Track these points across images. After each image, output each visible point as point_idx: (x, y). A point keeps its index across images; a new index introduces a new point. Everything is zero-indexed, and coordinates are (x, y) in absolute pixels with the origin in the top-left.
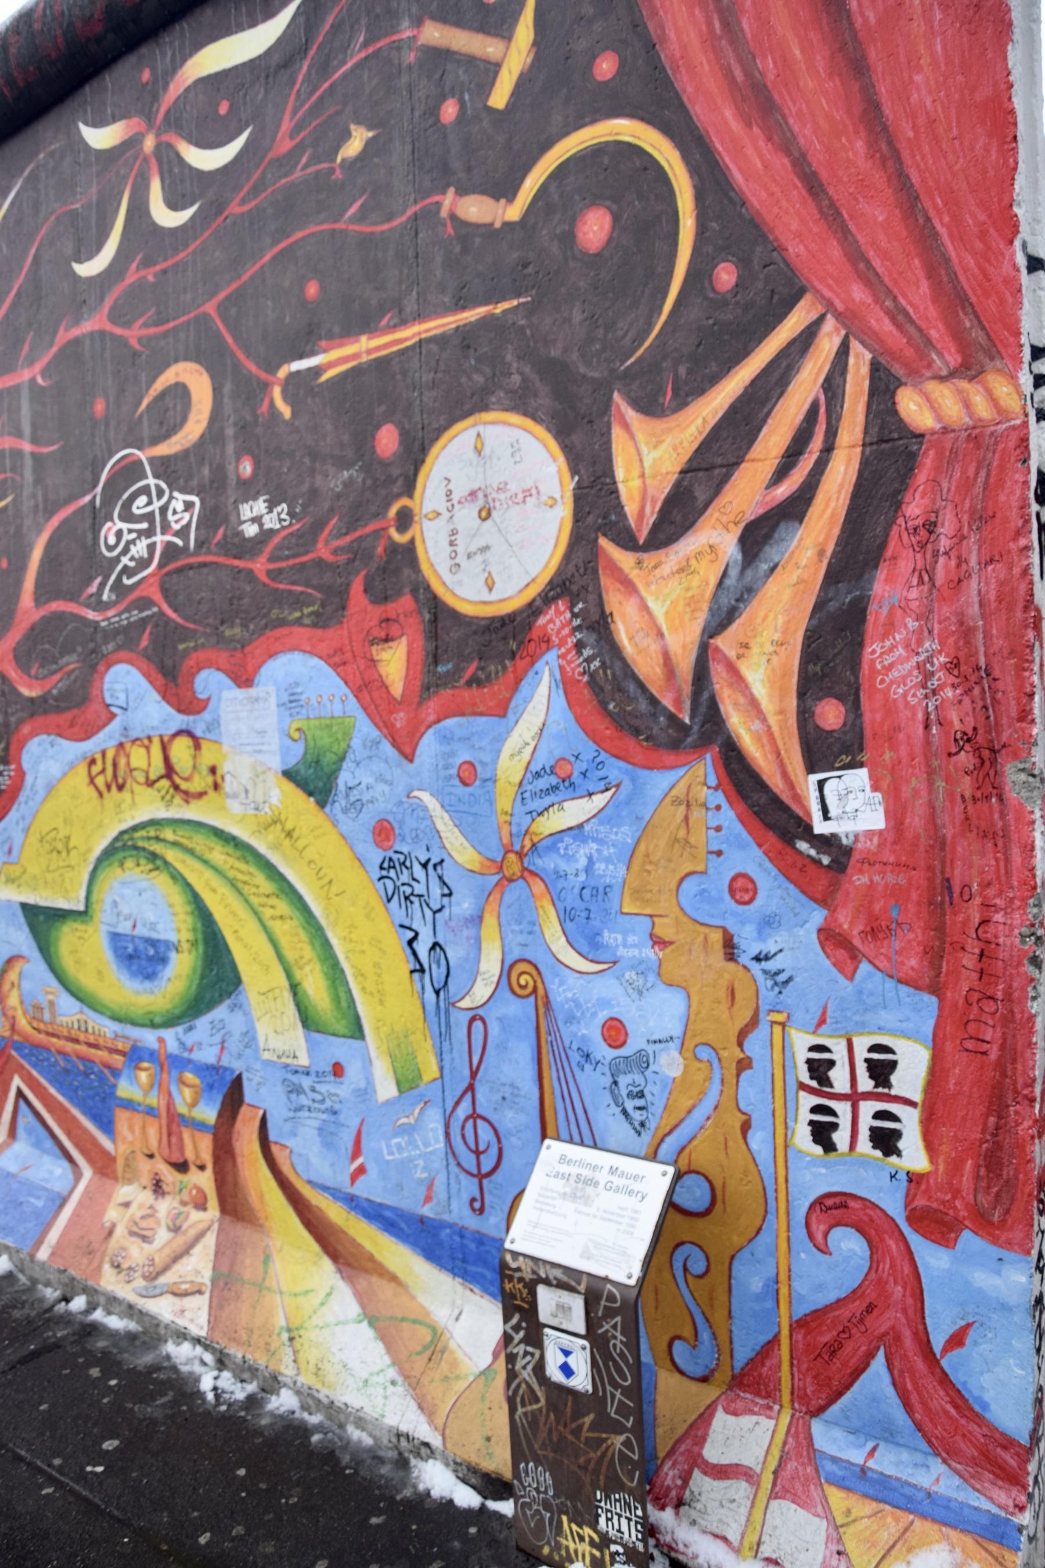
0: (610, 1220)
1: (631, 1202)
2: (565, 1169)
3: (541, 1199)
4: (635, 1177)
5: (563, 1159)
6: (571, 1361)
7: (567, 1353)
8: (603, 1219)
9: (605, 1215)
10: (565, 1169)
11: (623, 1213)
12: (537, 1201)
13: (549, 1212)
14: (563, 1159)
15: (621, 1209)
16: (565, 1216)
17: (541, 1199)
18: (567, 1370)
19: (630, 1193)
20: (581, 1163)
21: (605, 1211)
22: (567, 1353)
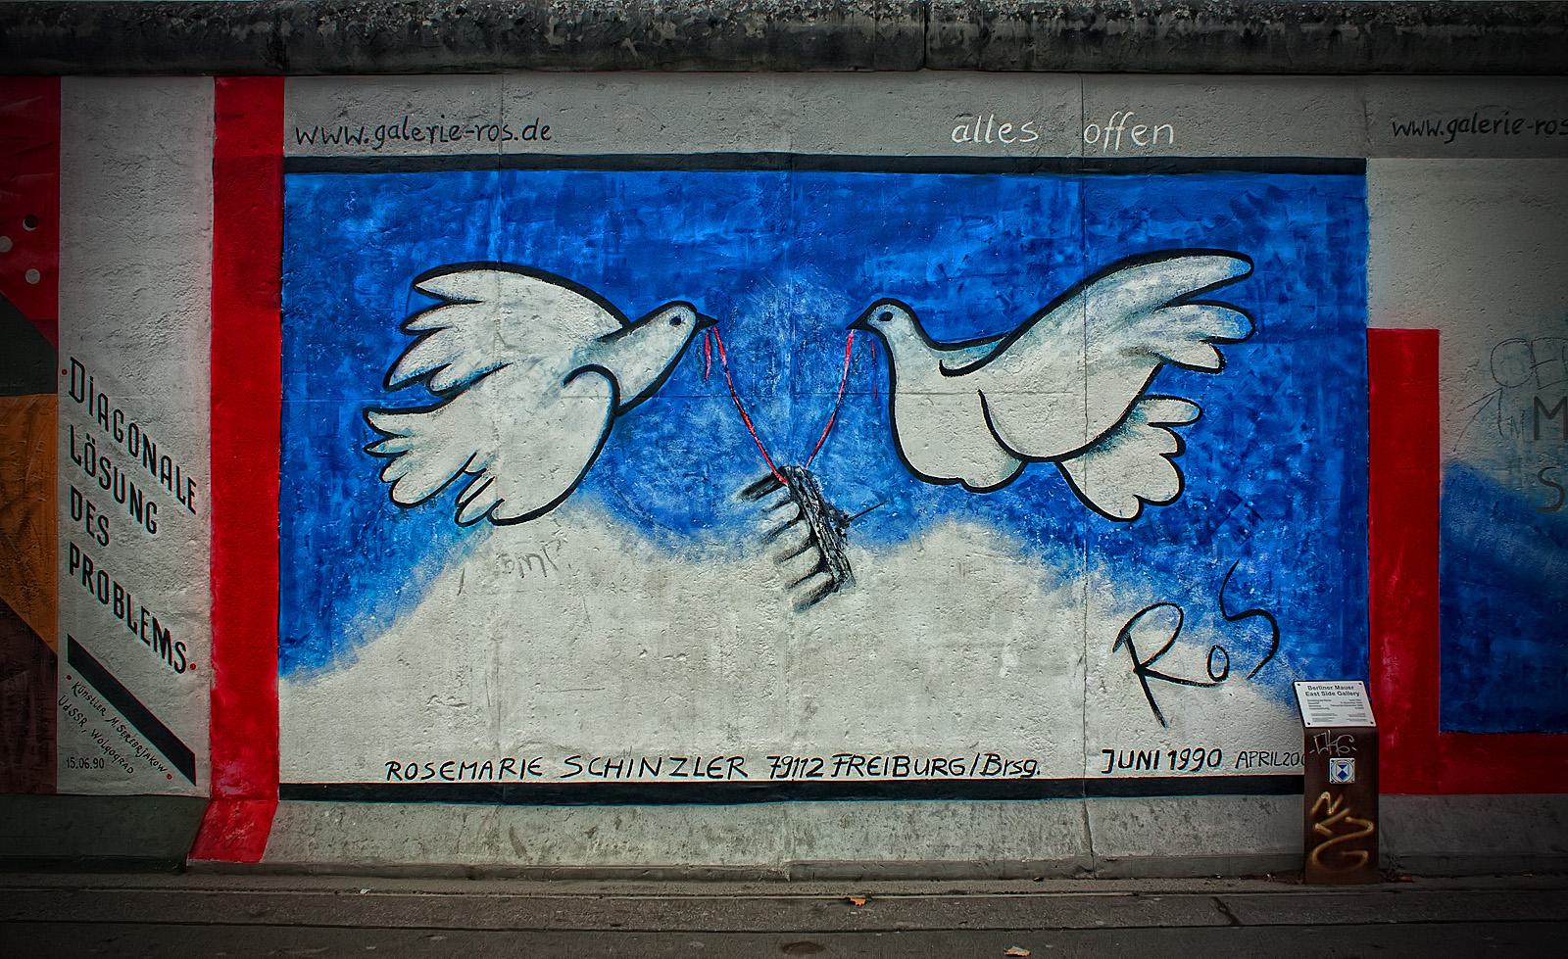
1: (1355, 697)
2: (1313, 691)
7: (1342, 767)
10: (1313, 691)
22: (1342, 767)
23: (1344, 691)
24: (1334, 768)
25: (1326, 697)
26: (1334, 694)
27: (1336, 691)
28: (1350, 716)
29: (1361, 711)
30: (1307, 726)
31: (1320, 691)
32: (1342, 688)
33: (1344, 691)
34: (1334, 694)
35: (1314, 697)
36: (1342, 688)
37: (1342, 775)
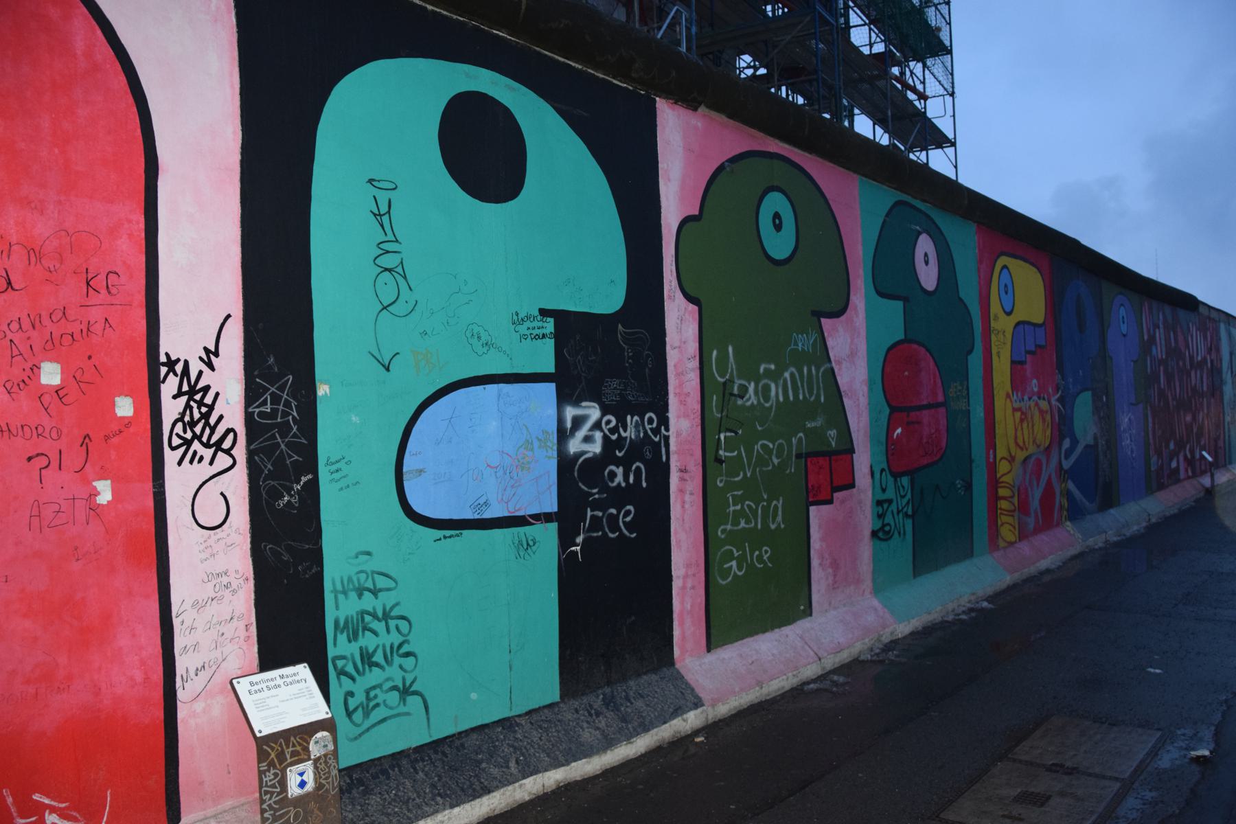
0: (300, 697)
1: (302, 685)
2: (256, 687)
3: (258, 706)
4: (294, 674)
5: (252, 684)
6: (305, 777)
7: (301, 774)
8: (295, 698)
9: (296, 696)
10: (256, 687)
11: (302, 691)
13: (267, 709)
15: (300, 690)
16: (277, 707)
17: (258, 706)
19: (298, 681)
20: (263, 681)
21: (294, 695)
22: (301, 774)
24: (293, 777)
25: (273, 692)
26: (279, 686)
28: (304, 710)
30: (258, 735)
31: (264, 686)
32: (287, 676)
34: (279, 686)
35: (259, 695)
36: (287, 676)
37: (302, 784)
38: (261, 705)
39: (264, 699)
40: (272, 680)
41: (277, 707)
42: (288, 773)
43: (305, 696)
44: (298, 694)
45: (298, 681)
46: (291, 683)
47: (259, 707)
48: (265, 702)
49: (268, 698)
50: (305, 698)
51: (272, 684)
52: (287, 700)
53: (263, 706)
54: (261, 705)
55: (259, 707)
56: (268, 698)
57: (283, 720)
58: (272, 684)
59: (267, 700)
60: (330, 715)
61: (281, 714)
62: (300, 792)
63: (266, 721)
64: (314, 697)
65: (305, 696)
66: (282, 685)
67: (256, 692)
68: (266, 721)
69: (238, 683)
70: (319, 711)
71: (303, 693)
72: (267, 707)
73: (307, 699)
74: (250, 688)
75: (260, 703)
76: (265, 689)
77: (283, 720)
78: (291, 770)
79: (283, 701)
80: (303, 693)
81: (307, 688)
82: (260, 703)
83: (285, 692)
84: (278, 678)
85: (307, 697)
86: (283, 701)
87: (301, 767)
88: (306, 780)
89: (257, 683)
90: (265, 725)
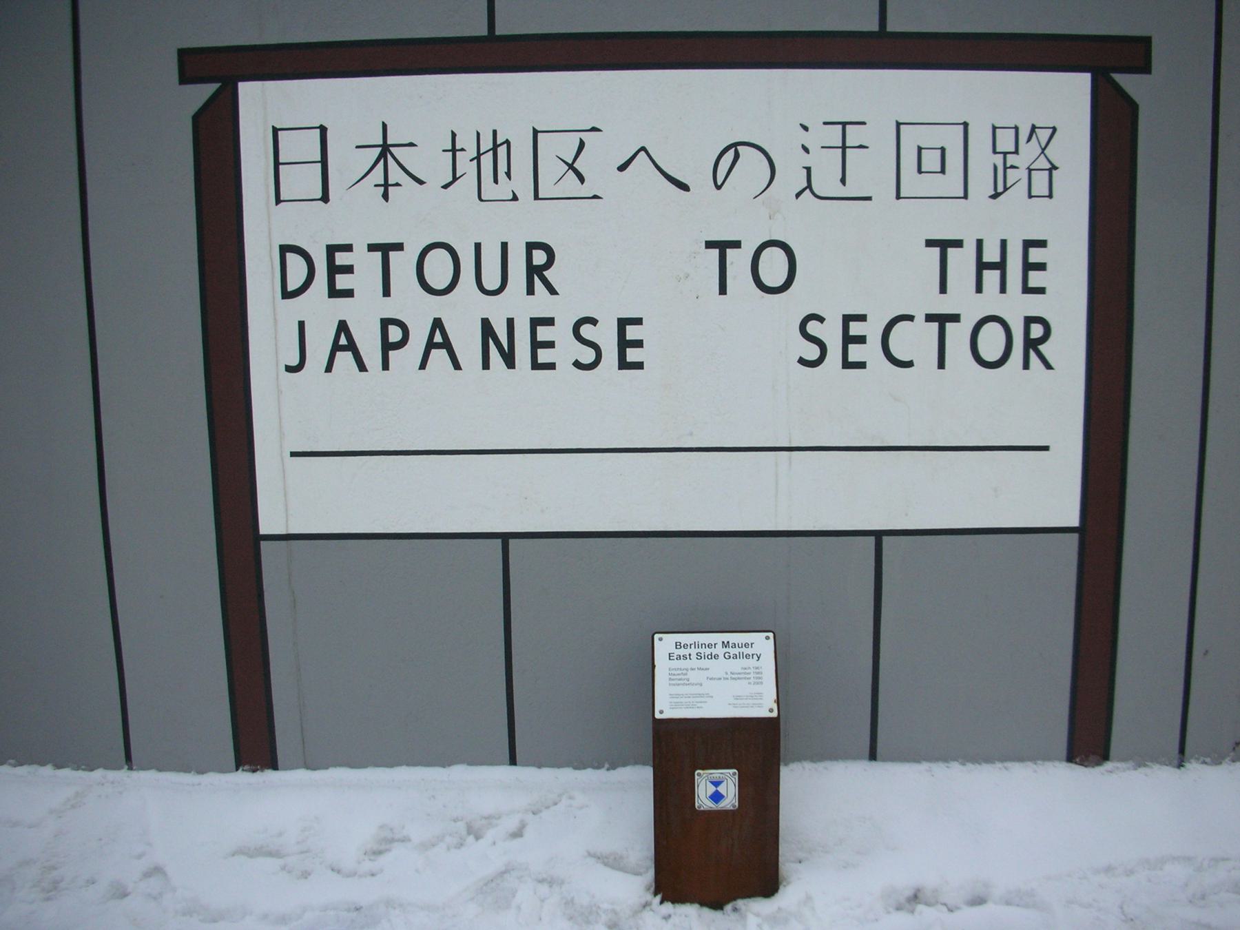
0: (739, 678)
1: (752, 662)
2: (682, 652)
3: (672, 677)
4: (746, 645)
5: (678, 645)
6: (722, 789)
7: (716, 784)
9: (733, 676)
10: (682, 652)
12: (670, 679)
13: (683, 684)
14: (678, 645)
15: (745, 669)
16: (701, 685)
17: (672, 677)
18: (717, 797)
19: (747, 656)
20: (696, 645)
22: (716, 784)
23: (736, 651)
25: (705, 663)
26: (716, 657)
27: (719, 650)
28: (737, 698)
29: (757, 688)
31: (693, 651)
32: (734, 646)
33: (736, 651)
34: (716, 657)
36: (734, 646)
37: (717, 797)
38: (678, 677)
39: (687, 670)
40: (709, 646)
41: (701, 685)
42: (696, 777)
43: (749, 678)
44: (739, 674)
45: (747, 656)
46: (735, 657)
47: (673, 680)
48: (686, 674)
49: (692, 669)
50: (747, 681)
51: (708, 651)
52: (720, 679)
53: (680, 680)
54: (678, 677)
55: (673, 680)
56: (692, 669)
57: (699, 705)
58: (708, 651)
59: (690, 672)
60: (775, 714)
61: (701, 695)
62: (713, 806)
63: (675, 700)
64: (762, 683)
65: (749, 678)
66: (721, 656)
67: (679, 657)
68: (675, 700)
69: (661, 639)
70: (760, 706)
71: (749, 673)
72: (686, 682)
73: (749, 683)
74: (673, 649)
75: (678, 674)
76: (694, 656)
77: (699, 705)
78: (699, 775)
79: (711, 679)
80: (749, 673)
81: (757, 668)
82: (678, 674)
83: (720, 667)
84: (720, 644)
85: (752, 680)
86: (711, 679)
87: (716, 773)
88: (724, 793)
89: (685, 646)
90: (669, 705)
